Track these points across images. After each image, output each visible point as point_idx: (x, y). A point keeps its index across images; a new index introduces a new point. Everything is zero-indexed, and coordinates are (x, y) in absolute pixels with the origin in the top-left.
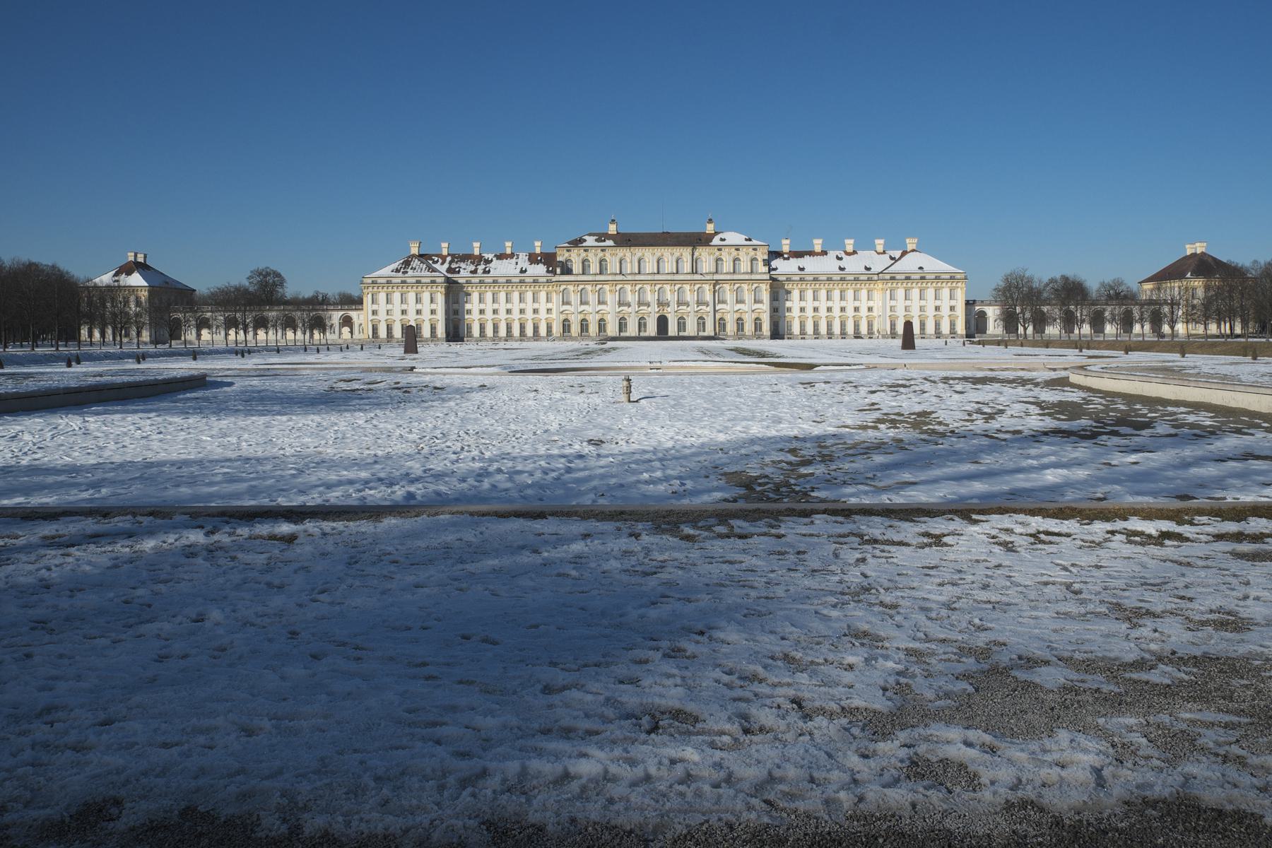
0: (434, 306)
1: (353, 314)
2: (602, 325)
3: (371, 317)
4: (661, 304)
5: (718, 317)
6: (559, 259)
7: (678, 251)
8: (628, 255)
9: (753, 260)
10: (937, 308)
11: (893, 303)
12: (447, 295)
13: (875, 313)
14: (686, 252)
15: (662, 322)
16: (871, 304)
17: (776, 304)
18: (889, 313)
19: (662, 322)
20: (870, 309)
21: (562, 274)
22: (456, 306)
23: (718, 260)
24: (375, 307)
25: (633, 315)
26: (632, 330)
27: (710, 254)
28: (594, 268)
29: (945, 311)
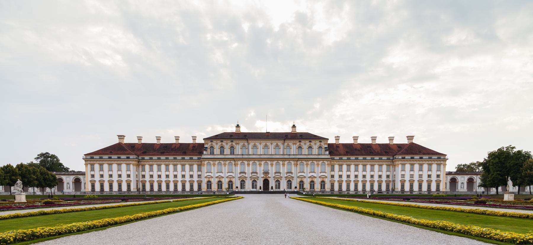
0: (128, 173)
1: (81, 177)
2: (230, 184)
3: (89, 178)
4: (266, 173)
5: (299, 180)
6: (206, 146)
7: (275, 143)
8: (246, 144)
9: (320, 147)
10: (429, 176)
11: (403, 173)
12: (138, 165)
13: (391, 179)
14: (280, 143)
15: (266, 182)
16: (388, 173)
17: (333, 173)
18: (400, 179)
19: (266, 182)
20: (388, 176)
21: (208, 155)
22: (143, 173)
23: (300, 147)
24: (92, 173)
25: (248, 179)
26: (248, 186)
27: (294, 144)
28: (227, 151)
29: (434, 178)
